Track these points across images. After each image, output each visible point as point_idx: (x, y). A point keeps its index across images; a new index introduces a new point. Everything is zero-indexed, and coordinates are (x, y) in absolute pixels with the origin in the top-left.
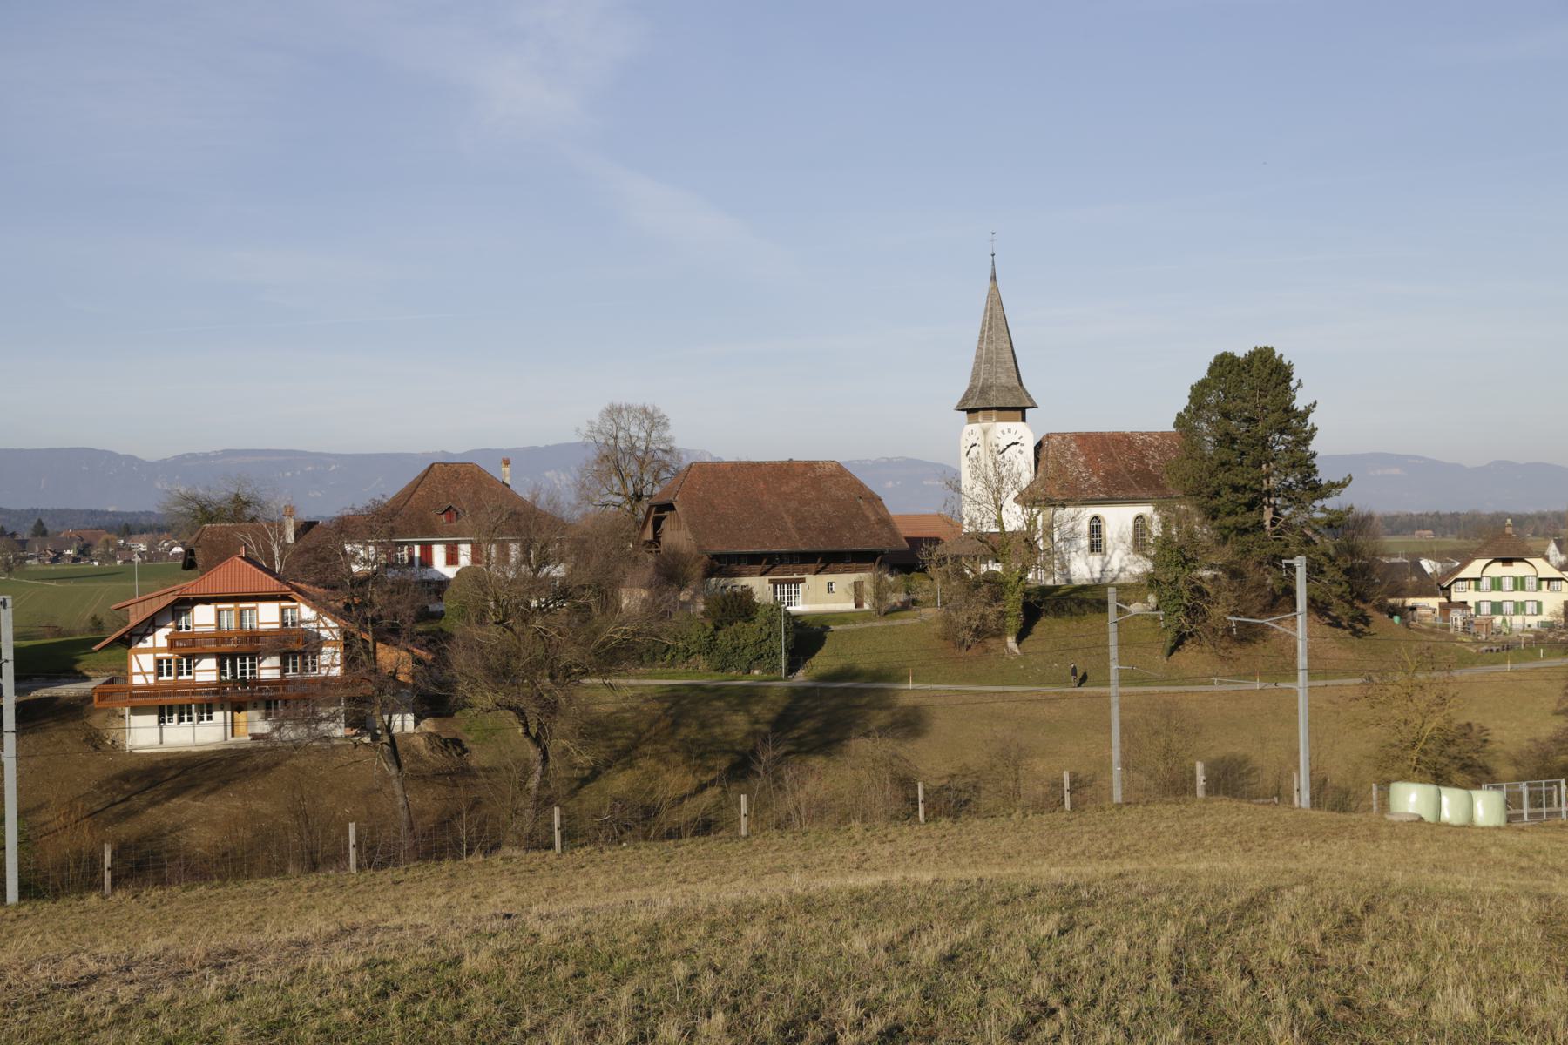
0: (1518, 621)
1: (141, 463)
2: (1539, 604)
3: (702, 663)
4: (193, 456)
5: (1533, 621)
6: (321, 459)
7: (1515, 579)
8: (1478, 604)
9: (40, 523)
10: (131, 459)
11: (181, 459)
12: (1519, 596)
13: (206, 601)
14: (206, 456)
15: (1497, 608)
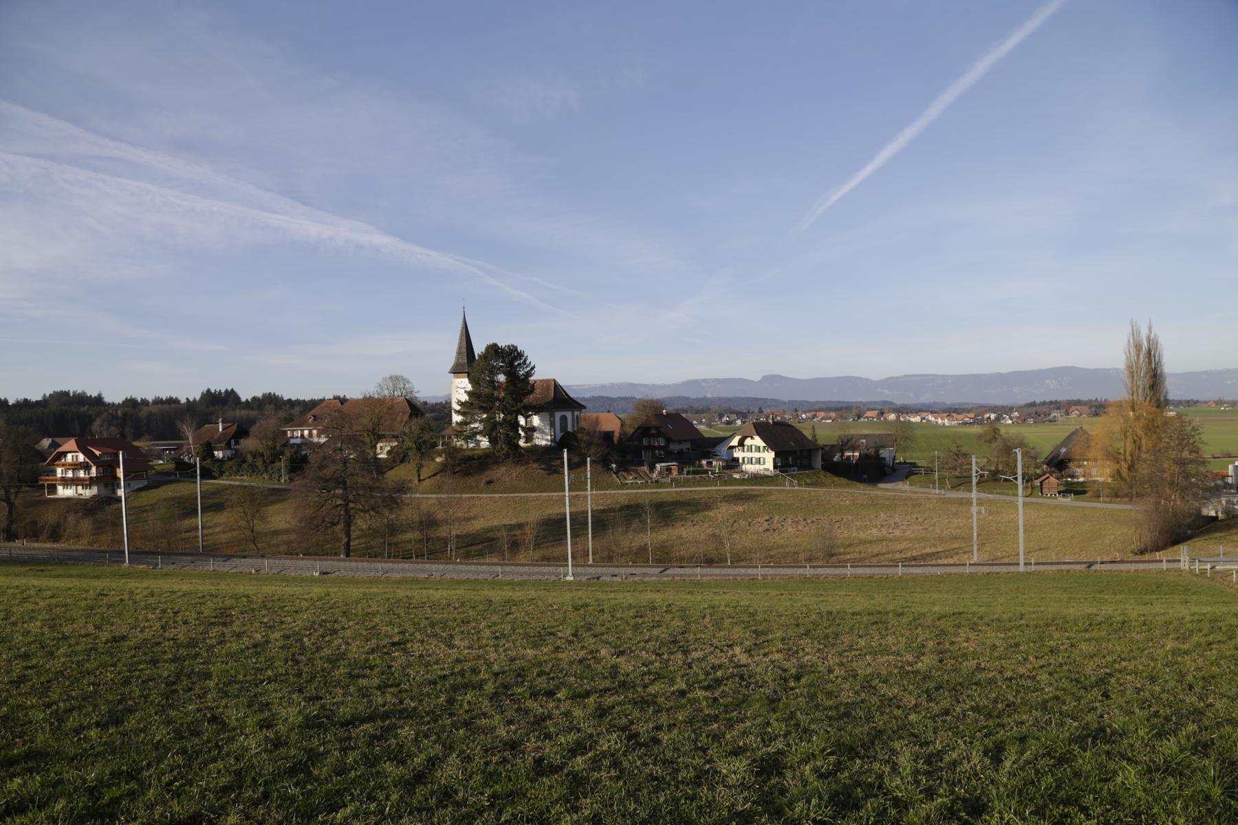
0: (758, 467)
1: (871, 381)
2: (764, 459)
3: (265, 476)
4: (892, 378)
5: (762, 467)
6: (944, 377)
7: (756, 446)
8: (744, 459)
9: (760, 408)
10: (867, 380)
11: (887, 379)
12: (757, 455)
13: (70, 452)
14: (897, 378)
15: (751, 461)
